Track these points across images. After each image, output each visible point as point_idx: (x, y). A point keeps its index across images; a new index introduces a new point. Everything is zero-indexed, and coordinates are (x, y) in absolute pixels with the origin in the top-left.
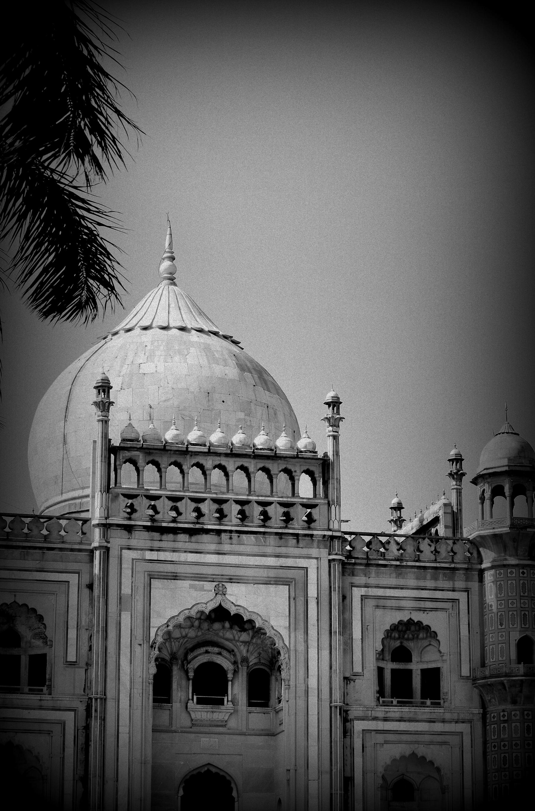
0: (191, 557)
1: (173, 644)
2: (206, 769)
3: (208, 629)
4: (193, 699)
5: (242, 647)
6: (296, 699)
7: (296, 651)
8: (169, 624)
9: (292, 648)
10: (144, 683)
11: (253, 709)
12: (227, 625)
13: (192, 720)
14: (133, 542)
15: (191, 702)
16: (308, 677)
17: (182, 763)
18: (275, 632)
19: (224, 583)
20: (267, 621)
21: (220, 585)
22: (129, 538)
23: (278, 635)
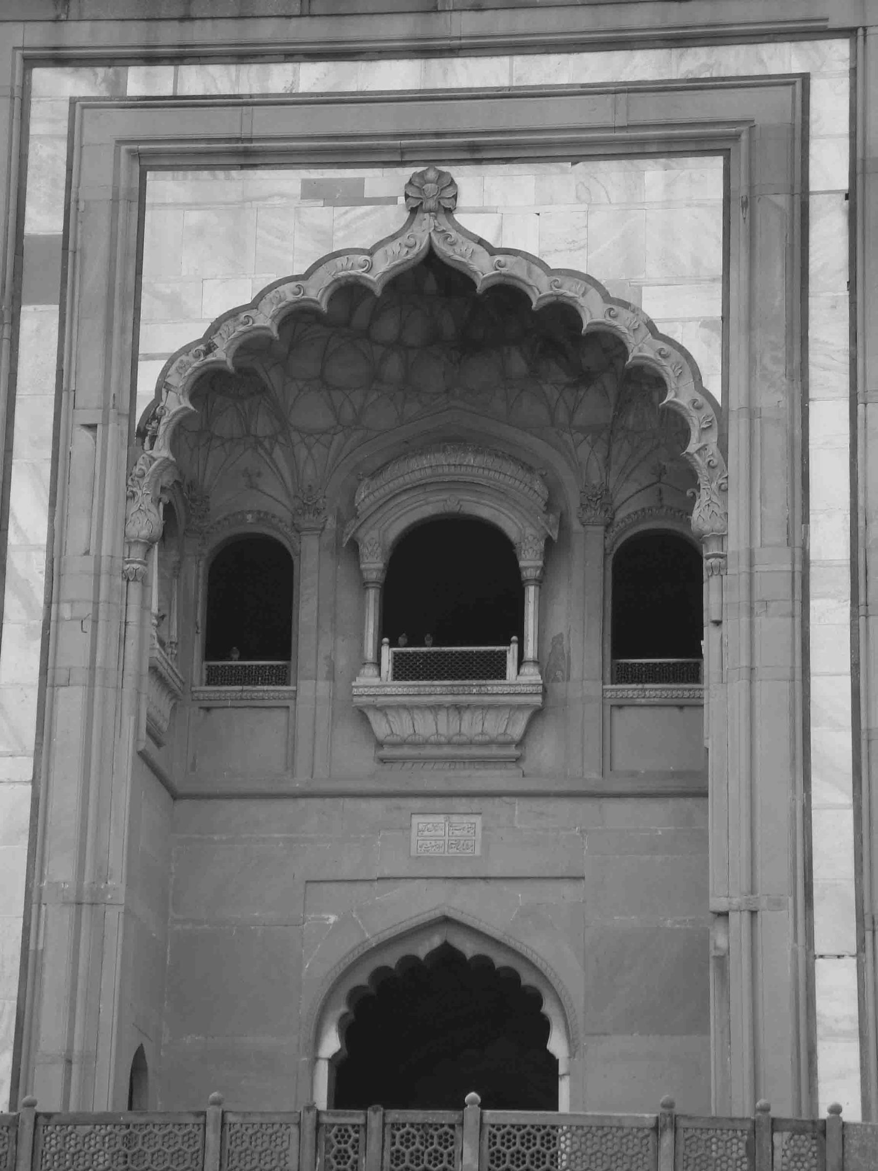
0: (312, 77)
1: (303, 453)
2: (436, 941)
3: (447, 391)
4: (378, 664)
5: (583, 451)
6: (751, 609)
7: (752, 413)
8: (216, 340)
9: (734, 405)
10: (104, 579)
11: (629, 690)
12: (518, 364)
13: (380, 745)
14: (78, 35)
15: (370, 671)
16: (806, 519)
17: (333, 919)
18: (660, 345)
19: (444, 169)
20: (626, 305)
21: (431, 175)
22: (57, 20)
23: (676, 355)
